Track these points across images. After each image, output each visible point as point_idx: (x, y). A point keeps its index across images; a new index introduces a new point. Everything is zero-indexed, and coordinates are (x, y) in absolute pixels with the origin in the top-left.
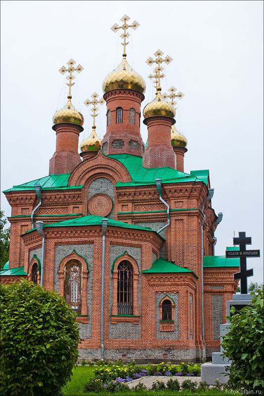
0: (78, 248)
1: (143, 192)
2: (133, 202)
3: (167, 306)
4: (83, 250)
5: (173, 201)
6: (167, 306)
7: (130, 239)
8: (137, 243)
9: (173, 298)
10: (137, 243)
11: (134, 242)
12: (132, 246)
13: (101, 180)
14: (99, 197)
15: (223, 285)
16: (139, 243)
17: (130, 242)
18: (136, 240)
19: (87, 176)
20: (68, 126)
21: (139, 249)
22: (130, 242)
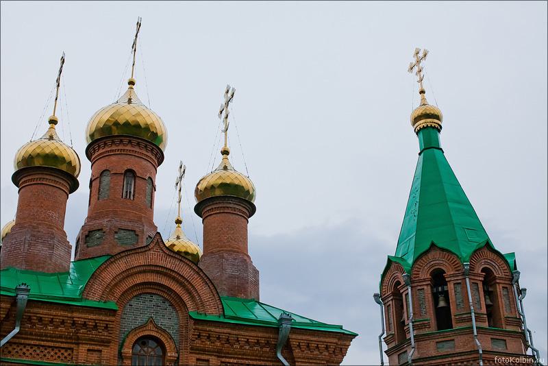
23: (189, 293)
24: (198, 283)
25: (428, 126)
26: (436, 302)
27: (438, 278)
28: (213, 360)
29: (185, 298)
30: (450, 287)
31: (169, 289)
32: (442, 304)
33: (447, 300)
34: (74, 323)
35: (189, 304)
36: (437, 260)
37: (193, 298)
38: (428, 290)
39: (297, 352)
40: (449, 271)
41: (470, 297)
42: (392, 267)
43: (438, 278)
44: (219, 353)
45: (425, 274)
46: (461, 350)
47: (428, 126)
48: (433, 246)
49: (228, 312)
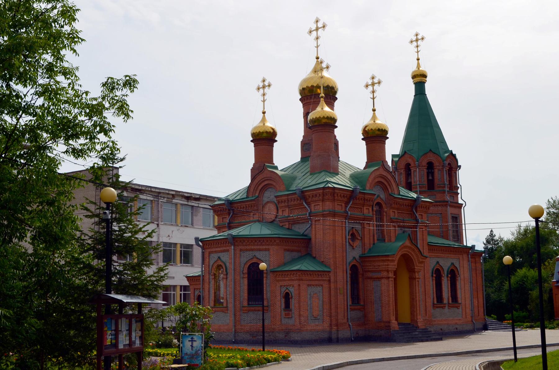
0: (221, 255)
1: (311, 196)
2: (288, 207)
3: (287, 297)
4: (225, 257)
5: (313, 205)
6: (287, 297)
7: (257, 245)
8: (264, 247)
9: (292, 290)
10: (264, 247)
11: (261, 247)
12: (260, 250)
13: (270, 190)
14: (269, 204)
15: (380, 271)
16: (267, 247)
17: (258, 247)
18: (263, 245)
19: (260, 188)
20: (264, 140)
21: (267, 252)
22: (258, 247)
23: (389, 185)
24: (392, 181)
25: (420, 81)
26: (428, 176)
27: (430, 166)
28: (396, 212)
29: (388, 187)
30: (436, 171)
31: (383, 183)
32: (430, 178)
33: (433, 176)
34: (364, 199)
35: (390, 190)
36: (431, 158)
37: (390, 187)
38: (426, 171)
39: (418, 209)
40: (436, 164)
41: (440, 176)
42: (406, 156)
43: (430, 166)
44: (398, 209)
45: (424, 163)
46: (439, 200)
47: (420, 81)
48: (430, 150)
49: (401, 193)
